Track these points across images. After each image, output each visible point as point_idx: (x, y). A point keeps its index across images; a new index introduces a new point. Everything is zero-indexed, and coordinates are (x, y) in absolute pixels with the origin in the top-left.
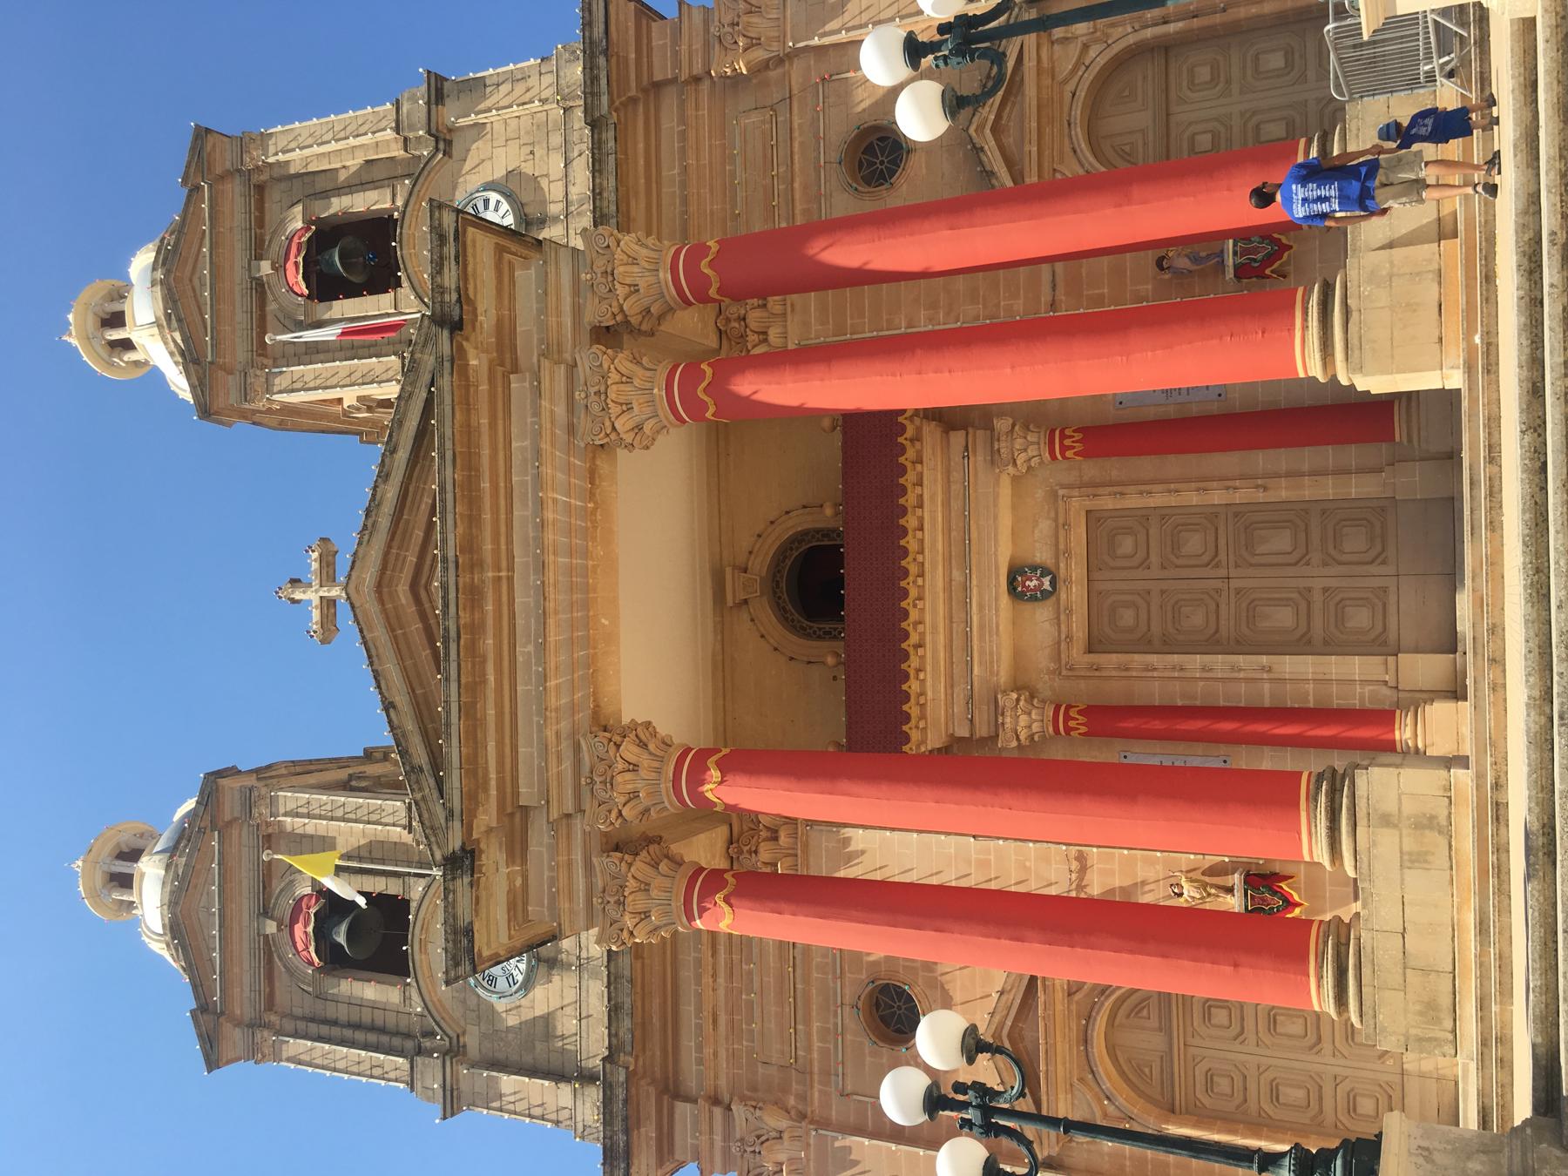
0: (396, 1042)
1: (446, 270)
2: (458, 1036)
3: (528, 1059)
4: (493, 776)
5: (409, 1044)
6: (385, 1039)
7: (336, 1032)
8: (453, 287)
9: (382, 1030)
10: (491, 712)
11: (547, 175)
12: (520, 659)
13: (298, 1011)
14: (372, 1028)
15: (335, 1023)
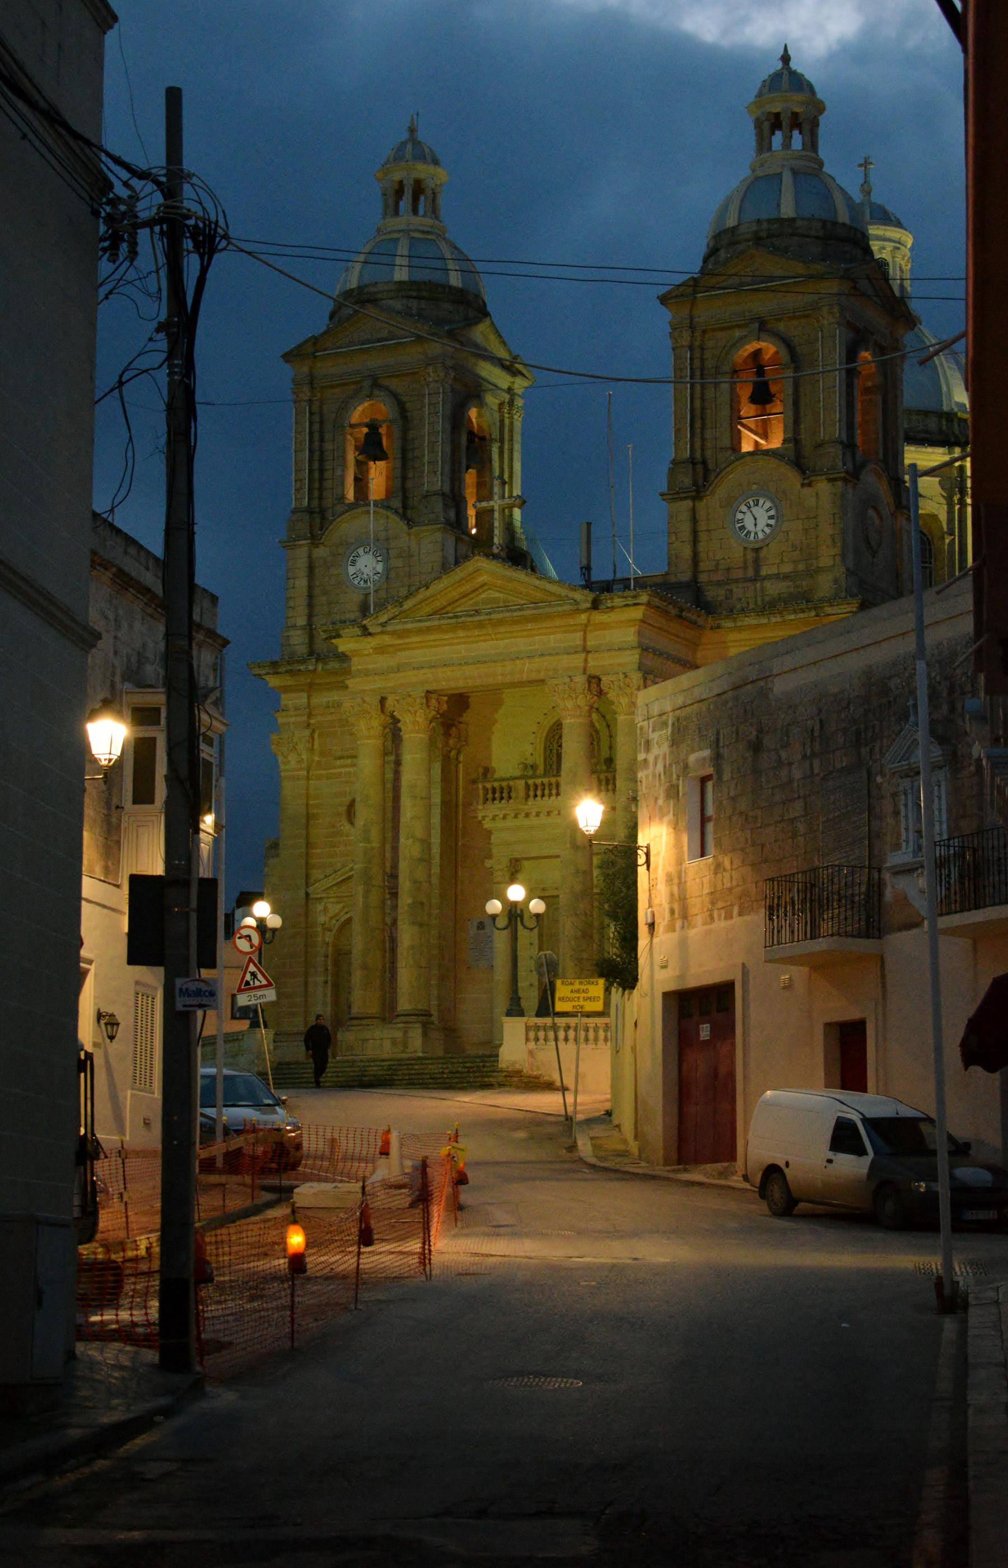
0: (316, 494)
1: (621, 600)
2: (323, 543)
3: (317, 591)
4: (407, 640)
5: (315, 503)
6: (317, 485)
7: (316, 444)
8: (614, 604)
9: (322, 479)
10: (432, 637)
11: (782, 562)
12: (459, 647)
13: (325, 408)
14: (322, 471)
15: (322, 440)
